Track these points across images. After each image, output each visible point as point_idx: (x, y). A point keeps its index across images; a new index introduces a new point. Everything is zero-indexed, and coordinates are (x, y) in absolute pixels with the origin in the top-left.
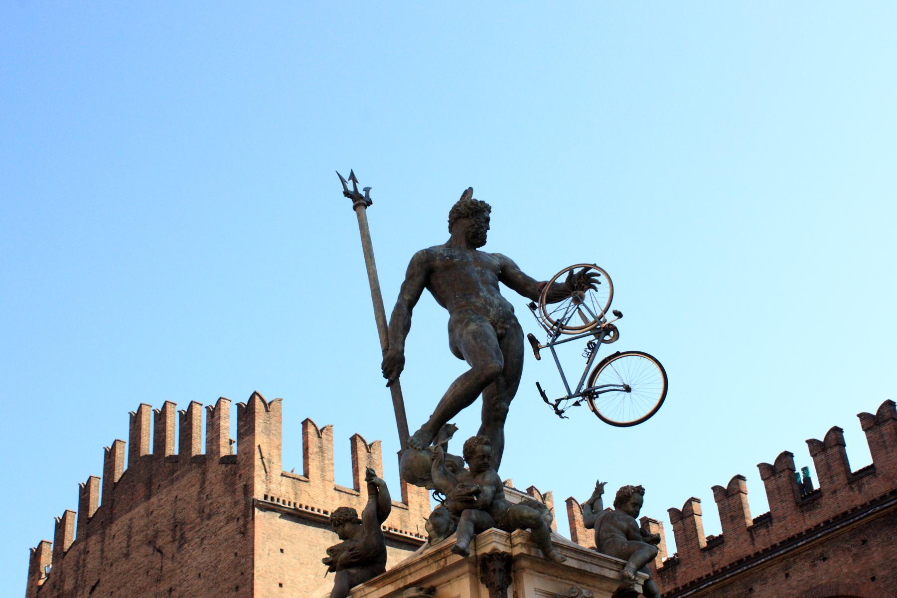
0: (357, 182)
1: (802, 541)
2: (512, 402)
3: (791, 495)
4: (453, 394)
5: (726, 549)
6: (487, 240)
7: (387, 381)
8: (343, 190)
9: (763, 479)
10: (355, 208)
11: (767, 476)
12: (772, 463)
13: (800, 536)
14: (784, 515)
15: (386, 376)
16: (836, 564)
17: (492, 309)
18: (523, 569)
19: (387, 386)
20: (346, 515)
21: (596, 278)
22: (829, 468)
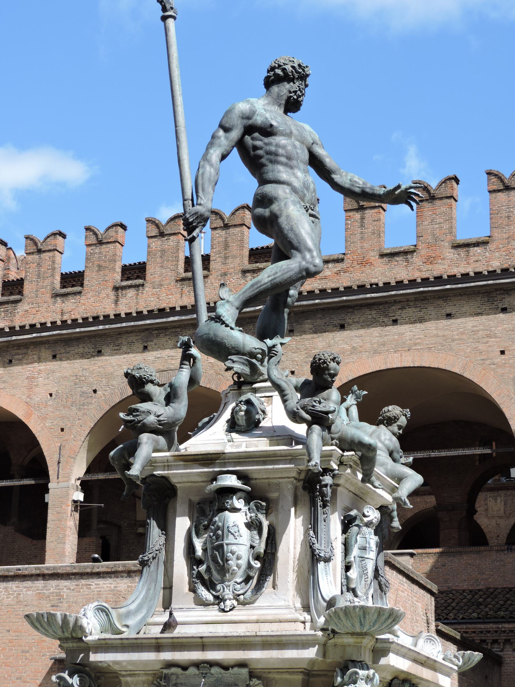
1: (174, 316)
5: (83, 299)
6: (301, 108)
11: (154, 234)
13: (173, 311)
17: (307, 194)
22: (226, 246)
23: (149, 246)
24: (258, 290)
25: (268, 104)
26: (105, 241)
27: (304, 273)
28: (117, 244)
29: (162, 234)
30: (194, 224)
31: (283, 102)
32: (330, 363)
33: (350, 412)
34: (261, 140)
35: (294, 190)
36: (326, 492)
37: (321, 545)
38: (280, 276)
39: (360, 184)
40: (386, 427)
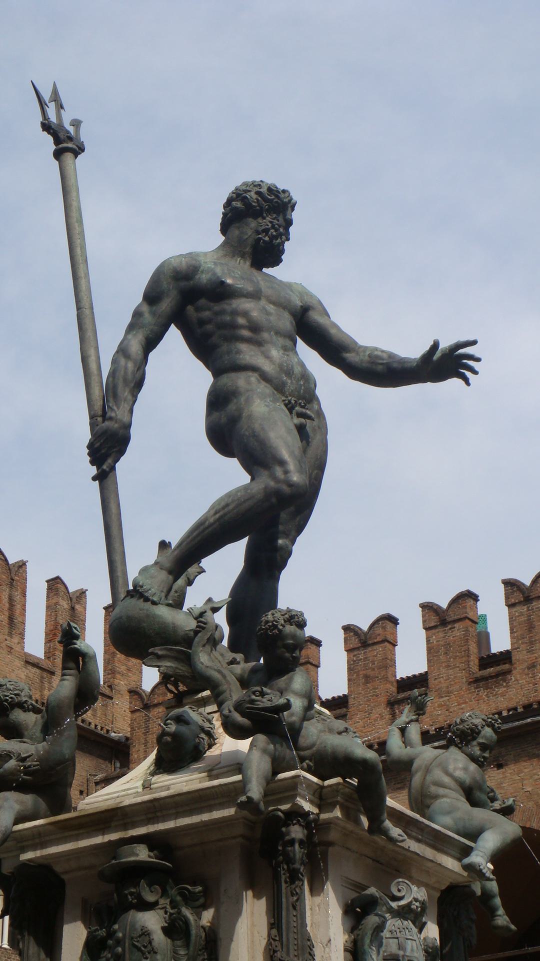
0: (62, 107)
2: (299, 539)
3: (464, 659)
4: (221, 517)
7: (94, 470)
8: (41, 119)
9: (424, 628)
10: (58, 155)
11: (433, 624)
12: (444, 605)
14: (448, 687)
15: (92, 463)
16: (517, 778)
18: (330, 844)
19: (94, 479)
20: (16, 695)
21: (471, 363)
23: (428, 641)
24: (199, 538)
25: (225, 256)
26: (371, 642)
27: (274, 500)
28: (386, 643)
29: (443, 623)
30: (103, 451)
31: (248, 249)
32: (284, 626)
33: (406, 734)
34: (209, 309)
35: (264, 377)
36: (291, 855)
37: (288, 954)
38: (233, 509)
39: (383, 359)
40: (460, 748)
